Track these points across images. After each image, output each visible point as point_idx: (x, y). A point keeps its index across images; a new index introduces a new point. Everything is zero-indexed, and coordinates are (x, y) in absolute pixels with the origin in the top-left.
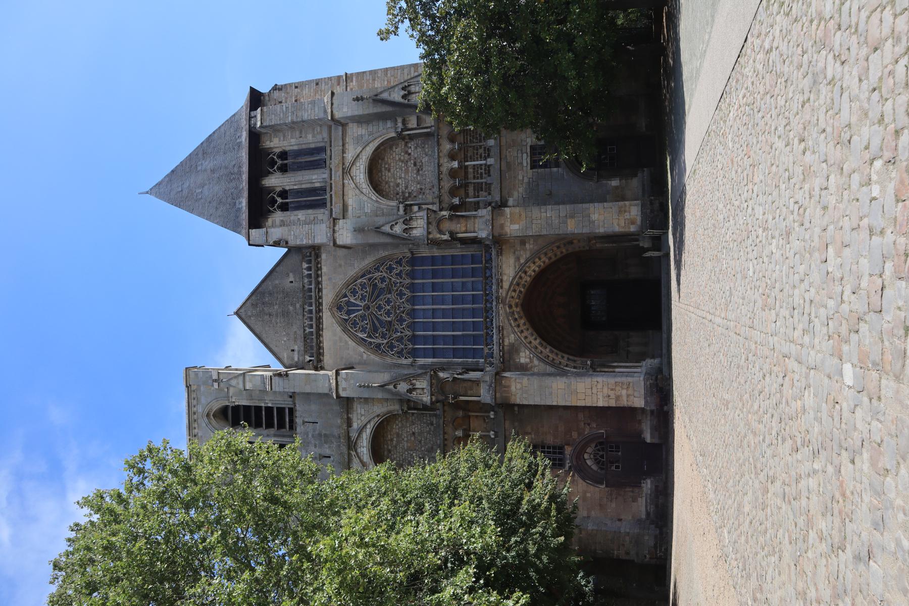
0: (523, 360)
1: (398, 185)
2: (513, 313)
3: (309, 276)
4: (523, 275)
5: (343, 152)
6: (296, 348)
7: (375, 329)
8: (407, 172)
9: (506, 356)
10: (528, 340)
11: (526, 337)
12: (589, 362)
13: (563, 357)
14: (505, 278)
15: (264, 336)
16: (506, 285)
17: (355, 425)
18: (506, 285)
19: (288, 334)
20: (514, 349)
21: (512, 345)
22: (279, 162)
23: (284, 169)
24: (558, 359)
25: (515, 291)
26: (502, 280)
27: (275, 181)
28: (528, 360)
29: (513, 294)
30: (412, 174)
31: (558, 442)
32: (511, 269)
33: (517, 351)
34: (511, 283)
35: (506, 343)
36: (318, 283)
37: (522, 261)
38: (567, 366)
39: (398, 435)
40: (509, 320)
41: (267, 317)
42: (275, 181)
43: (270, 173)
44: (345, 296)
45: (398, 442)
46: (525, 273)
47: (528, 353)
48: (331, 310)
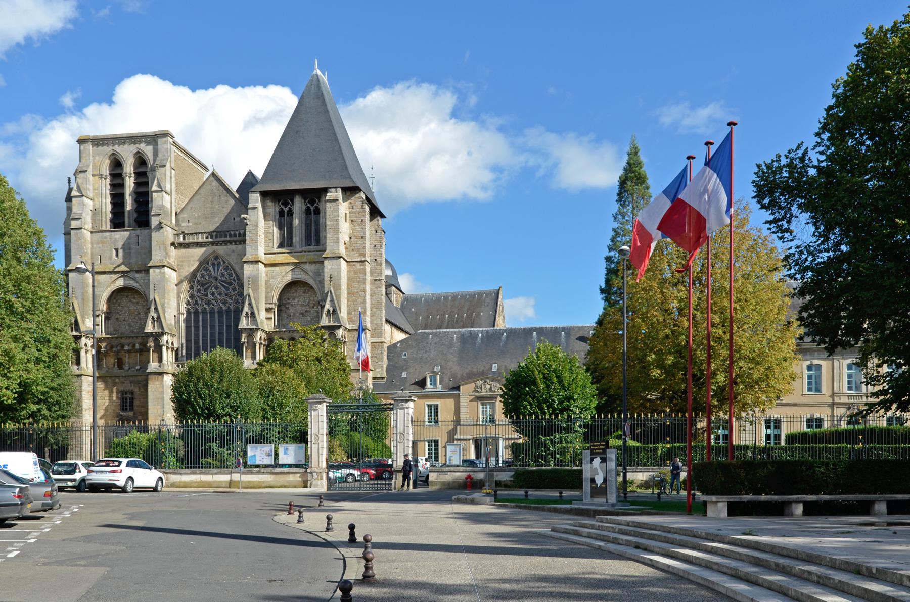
1: (294, 299)
3: (235, 236)
5: (310, 262)
6: (190, 224)
7: (203, 285)
8: (302, 305)
15: (198, 197)
17: (137, 275)
19: (199, 217)
22: (312, 208)
23: (308, 212)
27: (298, 205)
30: (300, 309)
31: (135, 408)
36: (230, 242)
39: (138, 303)
41: (210, 199)
42: (298, 205)
43: (305, 200)
44: (224, 262)
45: (133, 303)
48: (214, 252)
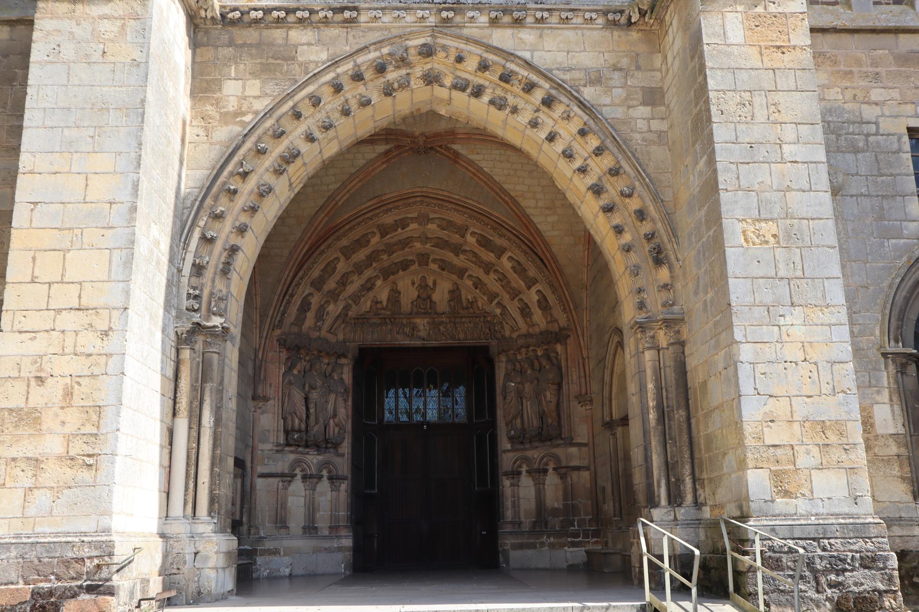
0: (231, 89)
2: (403, 62)
4: (538, 96)
9: (251, 35)
10: (306, 109)
11: (316, 101)
12: (217, 321)
13: (242, 230)
14: (527, 36)
16: (502, 38)
18: (502, 38)
20: (272, 62)
21: (288, 55)
24: (234, 211)
25: (484, 67)
26: (518, 23)
28: (232, 105)
29: (471, 64)
32: (561, 57)
33: (265, 71)
34: (509, 55)
35: (297, 35)
37: (588, 93)
38: (207, 240)
40: (379, 43)
46: (548, 102)
47: (261, 105)
